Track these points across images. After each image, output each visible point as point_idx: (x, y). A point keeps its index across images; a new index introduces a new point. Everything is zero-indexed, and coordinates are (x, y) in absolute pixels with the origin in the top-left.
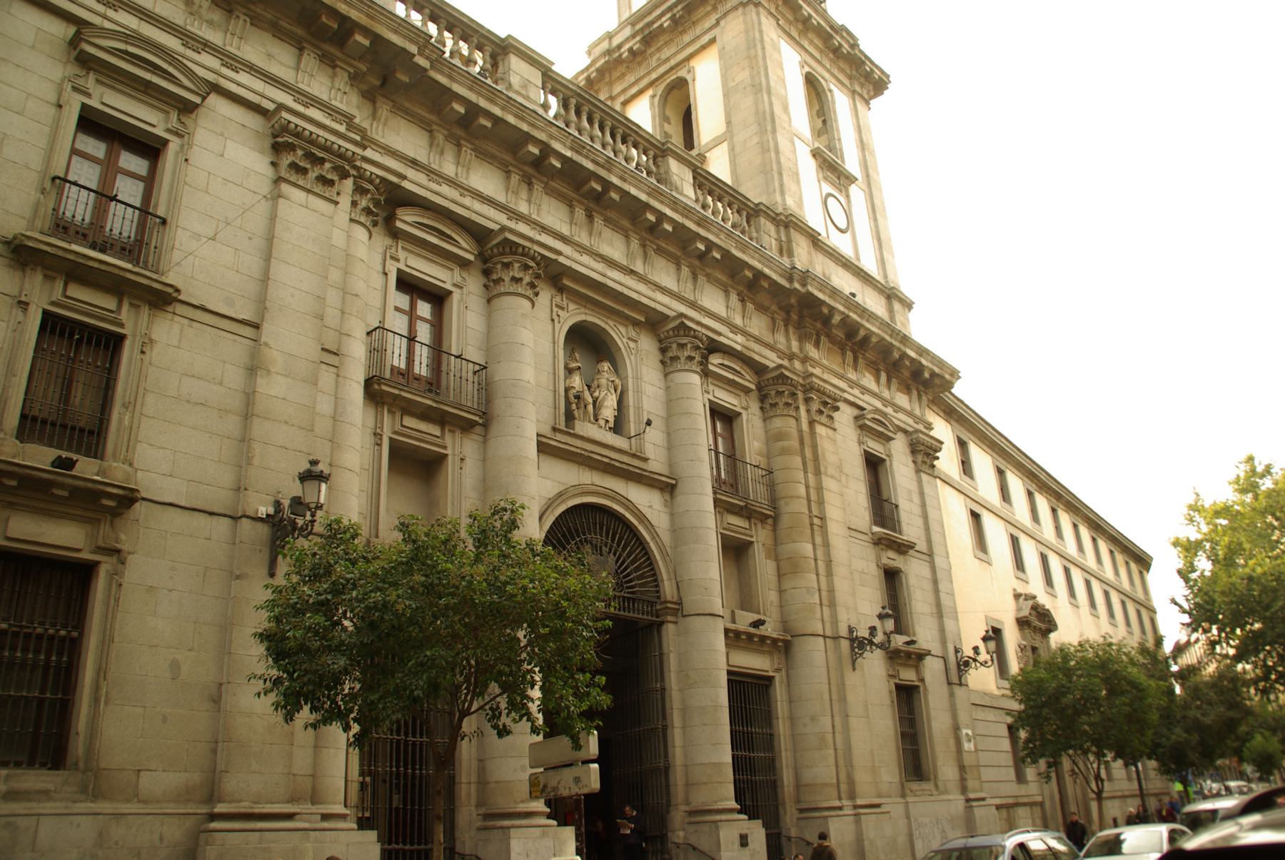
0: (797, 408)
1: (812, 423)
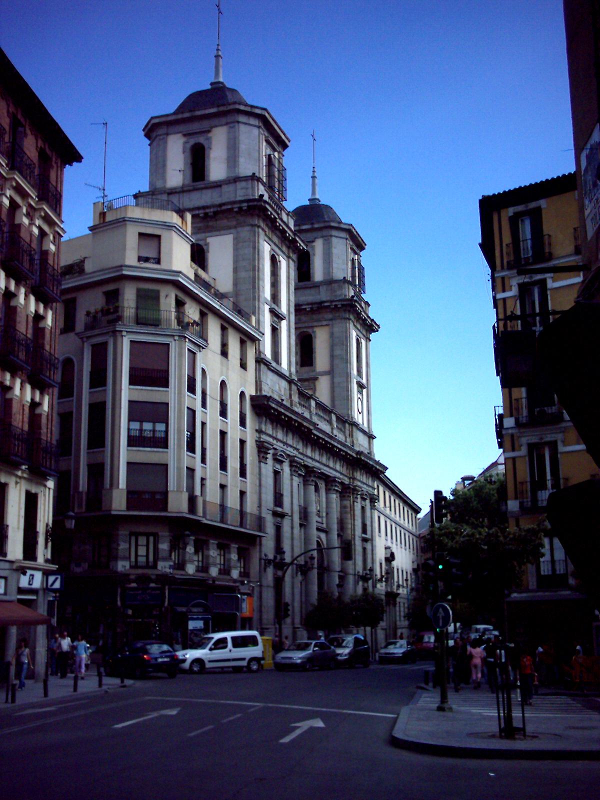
1: (354, 502)
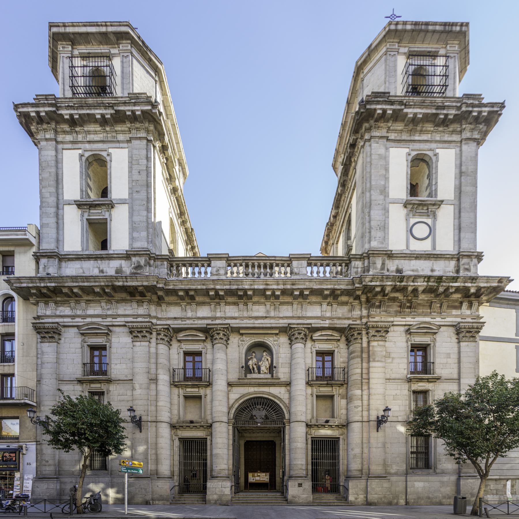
0: (361, 339)
1: (369, 342)
